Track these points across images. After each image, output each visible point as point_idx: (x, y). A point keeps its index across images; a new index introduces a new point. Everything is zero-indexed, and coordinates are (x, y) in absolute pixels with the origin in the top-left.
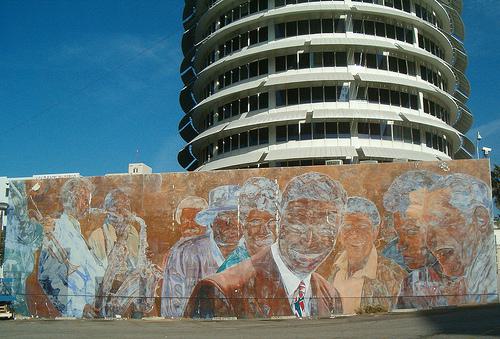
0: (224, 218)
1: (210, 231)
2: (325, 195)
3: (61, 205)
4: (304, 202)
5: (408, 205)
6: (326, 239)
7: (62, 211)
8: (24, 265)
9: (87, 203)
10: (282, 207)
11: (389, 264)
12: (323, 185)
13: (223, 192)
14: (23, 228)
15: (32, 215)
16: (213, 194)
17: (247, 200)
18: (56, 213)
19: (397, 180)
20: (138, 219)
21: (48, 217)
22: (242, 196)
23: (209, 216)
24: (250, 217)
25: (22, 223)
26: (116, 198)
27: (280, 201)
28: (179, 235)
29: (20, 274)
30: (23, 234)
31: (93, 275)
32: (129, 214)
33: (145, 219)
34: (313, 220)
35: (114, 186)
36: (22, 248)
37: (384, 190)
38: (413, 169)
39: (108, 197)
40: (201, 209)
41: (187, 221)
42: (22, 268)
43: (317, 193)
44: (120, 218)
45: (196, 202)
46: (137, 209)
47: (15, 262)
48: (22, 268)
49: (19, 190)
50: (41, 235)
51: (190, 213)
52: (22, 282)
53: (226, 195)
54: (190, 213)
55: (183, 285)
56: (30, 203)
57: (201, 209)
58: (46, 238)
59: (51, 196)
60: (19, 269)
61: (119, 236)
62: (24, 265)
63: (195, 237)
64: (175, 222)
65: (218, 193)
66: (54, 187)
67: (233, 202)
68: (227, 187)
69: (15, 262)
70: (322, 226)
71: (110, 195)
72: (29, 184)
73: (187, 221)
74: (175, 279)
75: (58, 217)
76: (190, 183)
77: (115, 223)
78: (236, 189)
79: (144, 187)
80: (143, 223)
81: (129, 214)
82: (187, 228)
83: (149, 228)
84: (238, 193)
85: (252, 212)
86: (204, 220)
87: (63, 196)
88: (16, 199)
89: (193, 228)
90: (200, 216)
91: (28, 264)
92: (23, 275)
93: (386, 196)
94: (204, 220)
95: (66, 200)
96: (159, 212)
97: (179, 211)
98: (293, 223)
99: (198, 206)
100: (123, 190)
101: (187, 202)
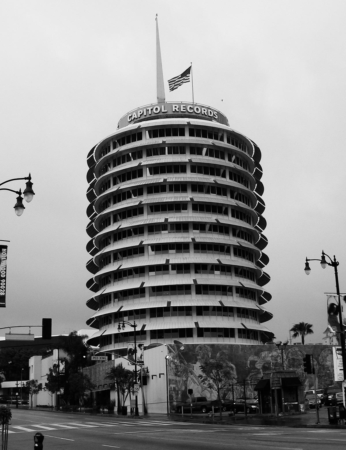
0: (266, 365)
1: (261, 370)
2: (300, 357)
3: (196, 358)
4: (293, 359)
5: (326, 362)
6: (301, 374)
7: (197, 361)
8: (180, 387)
9: (209, 357)
10: (286, 361)
11: (322, 384)
12: (299, 353)
13: (265, 354)
14: (178, 369)
15: (181, 362)
16: (261, 354)
19: (323, 352)
20: (232, 365)
22: (272, 356)
23: (261, 365)
24: (276, 365)
26: (221, 355)
27: (285, 358)
28: (249, 372)
29: (178, 391)
30: (178, 372)
32: (228, 363)
34: (297, 367)
35: (220, 350)
36: (178, 379)
37: (319, 356)
38: (328, 348)
39: (218, 355)
40: (257, 361)
41: (252, 366)
42: (178, 388)
43: (298, 356)
45: (255, 358)
46: (231, 360)
47: (174, 386)
48: (178, 388)
50: (187, 372)
51: (253, 363)
53: (266, 356)
54: (253, 363)
55: (253, 394)
57: (257, 361)
58: (190, 374)
59: (190, 353)
60: (177, 389)
62: (180, 387)
63: (255, 373)
64: (248, 366)
65: (263, 354)
67: (269, 359)
68: (266, 352)
69: (174, 386)
70: (300, 369)
71: (219, 353)
73: (252, 366)
74: (249, 391)
75: (195, 363)
78: (269, 353)
79: (234, 350)
80: (234, 367)
81: (228, 363)
82: (252, 369)
83: (237, 370)
84: (270, 355)
85: (276, 363)
86: (259, 366)
87: (197, 353)
89: (254, 369)
90: (257, 364)
91: (181, 387)
92: (180, 392)
93: (320, 358)
94: (259, 366)
95: (198, 355)
96: (240, 362)
97: (249, 362)
98: (290, 368)
99: (256, 360)
100: (224, 351)
101: (251, 358)
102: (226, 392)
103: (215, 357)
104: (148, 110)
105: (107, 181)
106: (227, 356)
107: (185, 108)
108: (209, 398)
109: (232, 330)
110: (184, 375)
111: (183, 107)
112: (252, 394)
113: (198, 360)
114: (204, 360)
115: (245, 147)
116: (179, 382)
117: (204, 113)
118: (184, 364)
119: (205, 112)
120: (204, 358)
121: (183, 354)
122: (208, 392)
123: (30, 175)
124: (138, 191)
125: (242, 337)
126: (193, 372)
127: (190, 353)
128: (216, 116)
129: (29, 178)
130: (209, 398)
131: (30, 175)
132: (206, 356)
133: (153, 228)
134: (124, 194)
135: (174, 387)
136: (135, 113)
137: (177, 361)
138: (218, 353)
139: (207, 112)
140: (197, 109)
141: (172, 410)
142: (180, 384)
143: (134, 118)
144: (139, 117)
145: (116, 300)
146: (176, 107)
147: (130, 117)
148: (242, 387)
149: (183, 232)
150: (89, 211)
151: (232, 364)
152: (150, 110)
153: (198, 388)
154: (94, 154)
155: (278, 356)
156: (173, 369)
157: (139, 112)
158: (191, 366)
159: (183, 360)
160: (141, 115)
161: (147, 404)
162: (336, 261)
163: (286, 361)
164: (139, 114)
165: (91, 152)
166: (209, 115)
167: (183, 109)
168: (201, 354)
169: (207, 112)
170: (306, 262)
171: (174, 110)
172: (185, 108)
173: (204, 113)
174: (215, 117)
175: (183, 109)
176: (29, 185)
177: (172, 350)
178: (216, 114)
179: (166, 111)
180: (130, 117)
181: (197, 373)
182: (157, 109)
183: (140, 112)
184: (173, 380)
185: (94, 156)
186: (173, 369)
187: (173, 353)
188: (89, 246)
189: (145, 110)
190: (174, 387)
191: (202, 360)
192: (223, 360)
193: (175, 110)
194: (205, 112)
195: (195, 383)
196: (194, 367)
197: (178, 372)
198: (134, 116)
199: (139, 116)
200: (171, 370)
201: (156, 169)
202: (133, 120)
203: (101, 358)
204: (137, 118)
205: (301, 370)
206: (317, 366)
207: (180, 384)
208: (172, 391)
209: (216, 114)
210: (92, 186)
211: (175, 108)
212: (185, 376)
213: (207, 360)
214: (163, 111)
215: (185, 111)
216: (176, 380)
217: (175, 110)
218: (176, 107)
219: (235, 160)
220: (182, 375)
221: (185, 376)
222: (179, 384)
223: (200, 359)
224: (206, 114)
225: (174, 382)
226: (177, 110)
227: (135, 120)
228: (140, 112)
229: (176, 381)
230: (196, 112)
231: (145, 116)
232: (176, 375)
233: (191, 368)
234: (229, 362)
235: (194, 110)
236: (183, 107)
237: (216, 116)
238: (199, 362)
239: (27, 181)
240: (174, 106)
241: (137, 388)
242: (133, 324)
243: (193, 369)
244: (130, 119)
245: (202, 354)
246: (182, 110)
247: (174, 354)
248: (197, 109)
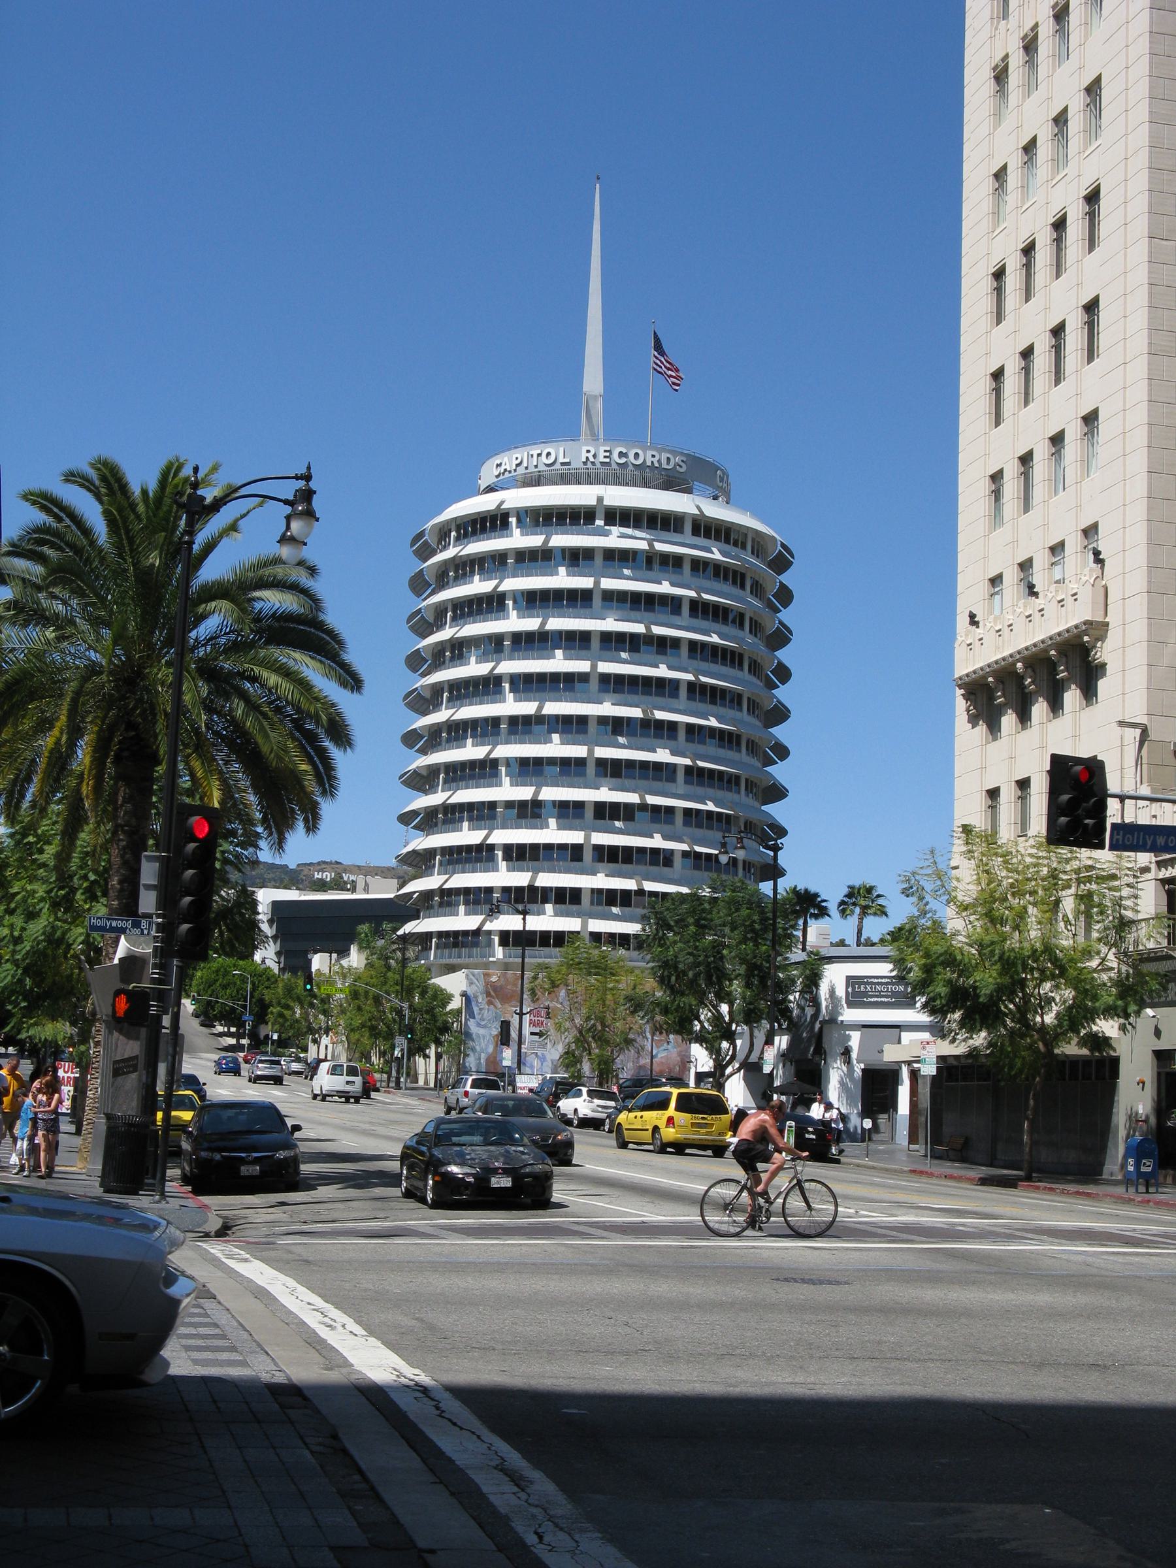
15: (490, 1003)
29: (480, 1055)
52: (482, 1061)
56: (488, 994)
88: (473, 986)
107: (608, 454)
111: (605, 451)
116: (484, 1037)
119: (655, 460)
121: (495, 988)
123: (309, 468)
124: (494, 645)
129: (307, 478)
131: (309, 468)
133: (521, 727)
139: (659, 461)
146: (588, 451)
166: (664, 466)
167: (605, 457)
169: (659, 461)
172: (608, 454)
175: (605, 457)
176: (307, 495)
179: (567, 460)
193: (587, 458)
194: (655, 460)
201: (534, 600)
211: (588, 455)
214: (561, 459)
215: (607, 460)
217: (587, 458)
218: (588, 451)
236: (605, 451)
237: (681, 466)
239: (301, 484)
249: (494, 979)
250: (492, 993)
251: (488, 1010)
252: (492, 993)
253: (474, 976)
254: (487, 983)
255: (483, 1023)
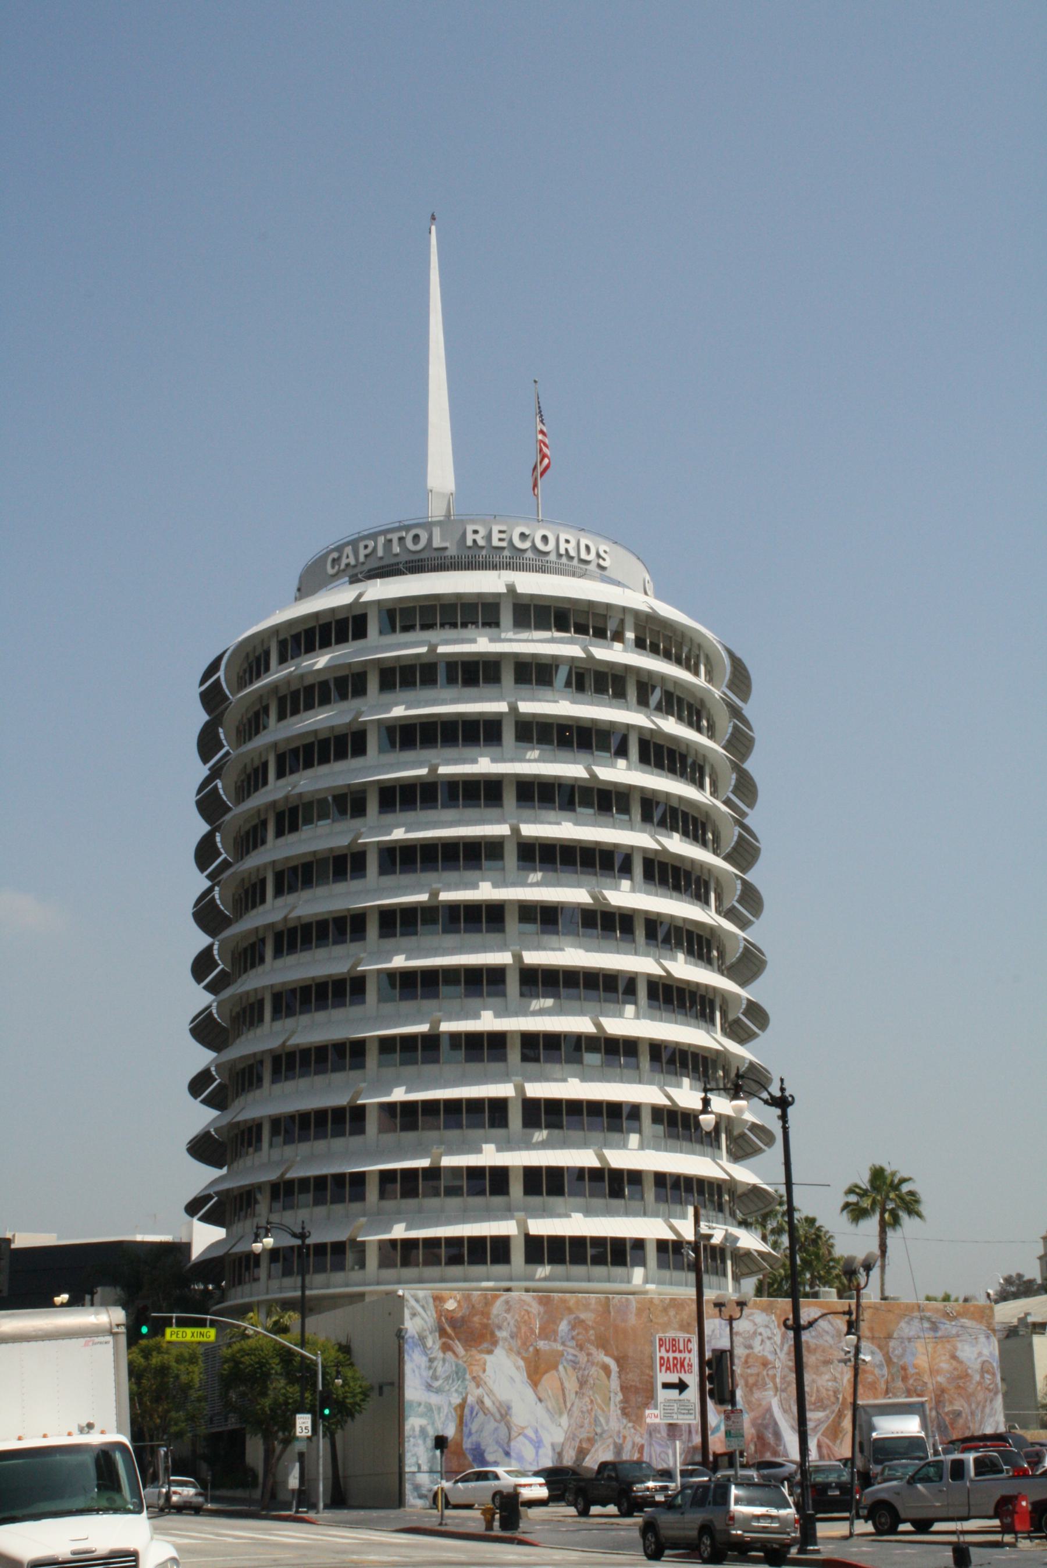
2: (828, 1338)
3: (493, 1334)
6: (831, 1393)
9: (532, 1331)
15: (446, 1348)
17: (741, 1340)
18: (485, 1345)
19: (903, 1324)
21: (474, 1352)
25: (431, 1360)
26: (573, 1328)
30: (435, 1377)
31: (547, 1440)
32: (593, 1350)
33: (617, 1360)
35: (570, 1310)
36: (434, 1399)
39: (563, 1327)
44: (582, 1358)
46: (603, 1344)
47: (423, 1421)
49: (423, 1307)
53: (717, 1332)
56: (442, 1332)
61: (582, 1383)
66: (479, 1306)
69: (423, 1421)
70: (827, 1377)
72: (438, 1299)
74: (660, 1445)
75: (490, 1352)
76: (672, 1313)
77: (575, 1365)
79: (612, 1314)
87: (496, 1321)
88: (418, 1321)
95: (500, 1328)
100: (583, 1316)
102: (584, 1445)
103: (555, 1332)
104: (390, 541)
105: (257, 763)
106: (591, 1332)
107: (503, 536)
108: (531, 1464)
109: (639, 1244)
110: (453, 1389)
111: (501, 532)
112: (667, 1454)
113: (501, 1343)
114: (519, 1342)
115: (698, 657)
116: (439, 1409)
117: (566, 550)
118: (454, 1353)
120: (517, 1336)
121: (453, 1321)
122: (527, 1442)
125: (671, 1267)
126: (481, 1379)
127: (476, 1319)
128: (604, 559)
130: (531, 1464)
132: (524, 1329)
134: (308, 806)
135: (421, 1426)
136: (348, 550)
137: (434, 1342)
138: (562, 1319)
140: (545, 539)
141: (414, 1498)
142: (440, 1418)
143: (348, 565)
144: (363, 563)
145: (280, 1139)
146: (476, 532)
147: (334, 560)
148: (635, 1429)
149: (487, 931)
150: (205, 853)
151: (606, 1355)
152: (395, 542)
153: (496, 1429)
154: (221, 673)
155: (755, 1333)
156: (419, 1368)
157: (361, 545)
158: (476, 1360)
159: (451, 1342)
160: (366, 556)
161: (345, 1477)
162: (306, 1231)
163: (781, 1349)
164: (362, 552)
165: (214, 667)
166: (584, 555)
167: (501, 540)
168: (509, 1324)
170: (255, 1230)
171: (469, 543)
172: (503, 536)
173: (566, 550)
174: (601, 562)
175: (501, 540)
177: (420, 1310)
178: (605, 552)
180: (334, 560)
181: (494, 1382)
182: (416, 538)
183: (366, 547)
184: (420, 1404)
185: (222, 679)
186: (419, 1368)
187: (423, 1319)
188: (202, 965)
189: (381, 540)
190: (421, 1426)
191: (513, 1343)
192: (579, 1342)
193: (475, 541)
195: (489, 1415)
196: (485, 1364)
197: (435, 1377)
198: (348, 557)
199: (362, 559)
200: (414, 1372)
202: (344, 570)
203: (195, 1335)
204: (355, 566)
205: (828, 1380)
206: (882, 1370)
207: (440, 1418)
208: (414, 1437)
209: (605, 552)
210: (215, 773)
212: (456, 1391)
213: (528, 1344)
215: (504, 544)
216: (430, 1404)
217: (475, 541)
218: (476, 532)
219: (660, 702)
220: (447, 1387)
221: (456, 1391)
222: (436, 1417)
223: (505, 1339)
224: (572, 553)
225: (422, 1409)
226: (481, 542)
227: (350, 572)
228: (366, 547)
229: (429, 1408)
230: (540, 545)
231: (381, 558)
232: (429, 1387)
233: (475, 1368)
234: (598, 1349)
235: (533, 542)
236: (501, 532)
237: (604, 559)
238: (503, 1347)
240: (470, 529)
241: (304, 1426)
242: (298, 1230)
243: (484, 1371)
244: (333, 567)
245: (512, 1322)
246: (495, 542)
247: (425, 1322)
248: (545, 539)
249: (451, 1305)
250: (449, 1330)
251: (444, 1360)
252: (449, 1330)
253: (417, 1300)
254: (440, 1313)
255: (436, 1384)
